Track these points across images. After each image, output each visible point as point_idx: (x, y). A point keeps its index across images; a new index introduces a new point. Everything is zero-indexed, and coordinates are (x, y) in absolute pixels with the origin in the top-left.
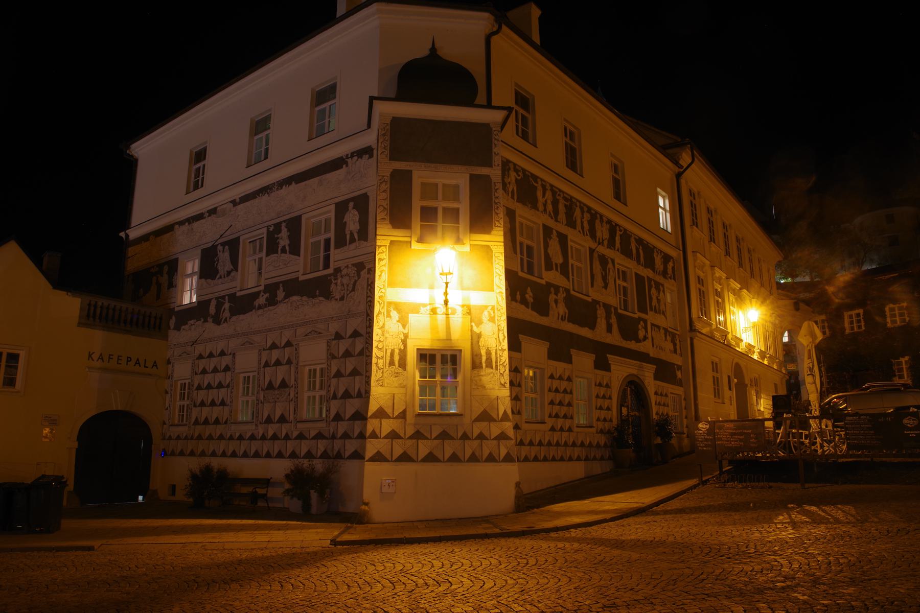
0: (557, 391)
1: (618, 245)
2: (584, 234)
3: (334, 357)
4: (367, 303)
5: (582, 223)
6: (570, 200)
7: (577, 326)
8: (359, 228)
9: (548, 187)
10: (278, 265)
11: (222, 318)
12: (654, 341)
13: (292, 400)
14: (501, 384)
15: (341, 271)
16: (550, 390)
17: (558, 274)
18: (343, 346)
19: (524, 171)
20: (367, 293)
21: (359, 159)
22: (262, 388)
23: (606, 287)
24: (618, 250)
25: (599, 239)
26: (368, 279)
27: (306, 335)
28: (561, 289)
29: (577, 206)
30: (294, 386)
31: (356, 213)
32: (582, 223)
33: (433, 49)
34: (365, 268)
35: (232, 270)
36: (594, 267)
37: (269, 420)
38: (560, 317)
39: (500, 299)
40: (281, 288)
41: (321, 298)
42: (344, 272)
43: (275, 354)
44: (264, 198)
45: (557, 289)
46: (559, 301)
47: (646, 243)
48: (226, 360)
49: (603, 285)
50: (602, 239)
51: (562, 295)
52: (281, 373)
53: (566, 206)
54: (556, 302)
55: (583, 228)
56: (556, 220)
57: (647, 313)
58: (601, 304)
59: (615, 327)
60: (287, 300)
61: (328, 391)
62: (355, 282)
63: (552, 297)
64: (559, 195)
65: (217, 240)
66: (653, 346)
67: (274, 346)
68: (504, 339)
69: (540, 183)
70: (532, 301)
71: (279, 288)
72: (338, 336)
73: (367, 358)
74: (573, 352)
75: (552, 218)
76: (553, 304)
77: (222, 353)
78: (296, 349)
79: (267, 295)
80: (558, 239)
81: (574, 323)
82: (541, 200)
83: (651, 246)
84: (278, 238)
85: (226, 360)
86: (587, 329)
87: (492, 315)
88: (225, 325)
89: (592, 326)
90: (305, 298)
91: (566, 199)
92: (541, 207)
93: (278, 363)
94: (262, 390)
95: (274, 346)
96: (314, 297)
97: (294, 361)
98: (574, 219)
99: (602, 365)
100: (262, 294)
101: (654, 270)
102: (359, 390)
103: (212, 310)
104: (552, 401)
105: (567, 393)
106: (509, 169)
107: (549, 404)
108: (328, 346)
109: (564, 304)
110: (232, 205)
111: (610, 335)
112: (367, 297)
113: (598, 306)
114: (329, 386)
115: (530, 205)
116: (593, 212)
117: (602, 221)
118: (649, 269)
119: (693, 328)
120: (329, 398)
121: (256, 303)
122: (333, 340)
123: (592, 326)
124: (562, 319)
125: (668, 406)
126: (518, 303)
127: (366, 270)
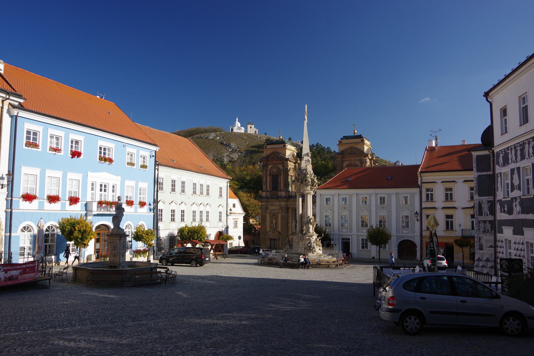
0: (517, 249)
5: (529, 151)
7: (525, 214)
16: (514, 249)
32: (529, 151)
45: (516, 198)
46: (517, 205)
54: (516, 206)
63: (514, 203)
74: (524, 229)
75: (515, 163)
76: (514, 207)
81: (524, 214)
82: (510, 157)
86: (531, 214)
92: (510, 161)
104: (515, 254)
105: (522, 251)
109: (519, 205)
124: (518, 214)
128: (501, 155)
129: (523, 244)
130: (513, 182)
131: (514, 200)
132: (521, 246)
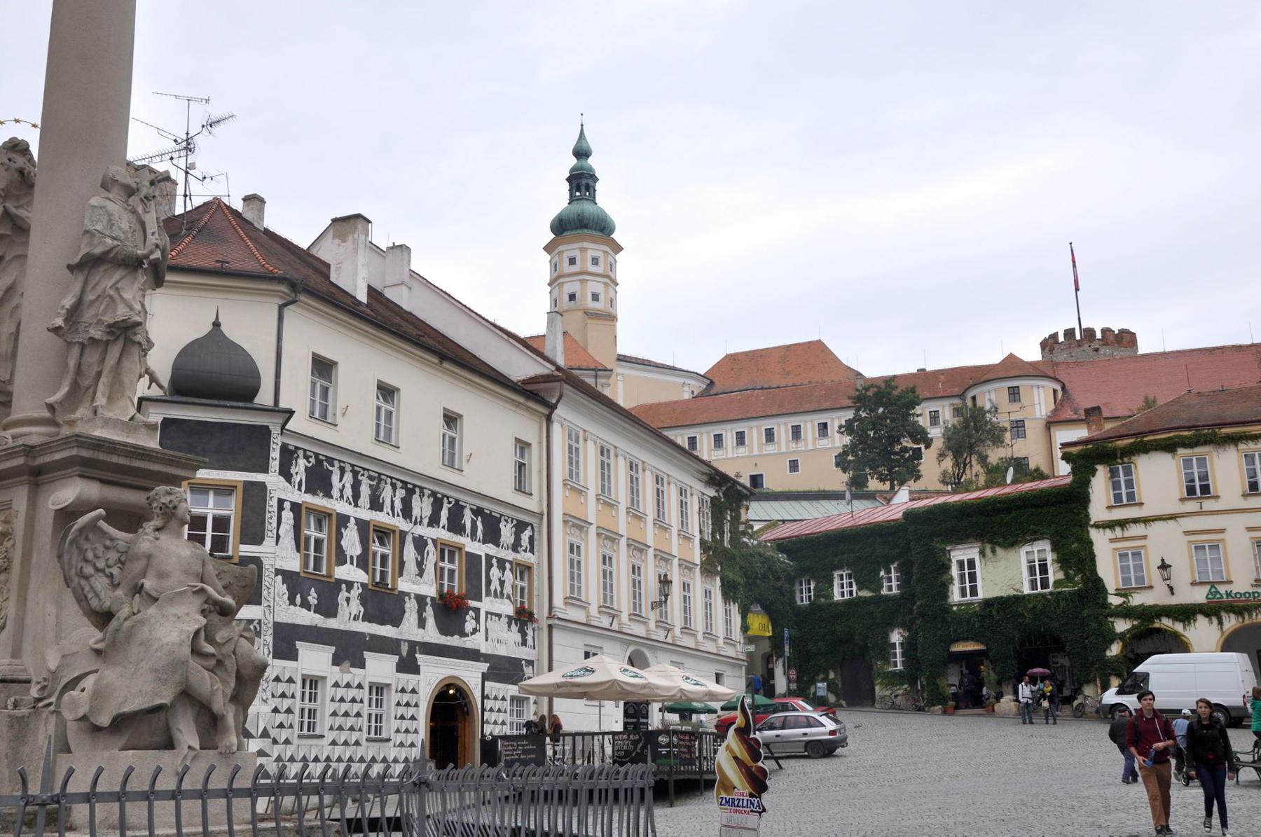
1: (444, 519)
2: (394, 516)
5: (392, 502)
6: (380, 477)
9: (348, 468)
12: (489, 633)
14: (263, 700)
16: (333, 700)
17: (353, 568)
19: (317, 455)
23: (421, 574)
24: (443, 527)
25: (416, 518)
28: (356, 584)
29: (386, 484)
32: (392, 502)
33: (216, 324)
36: (405, 553)
38: (352, 616)
39: (267, 613)
45: (350, 585)
47: (488, 512)
49: (418, 572)
50: (421, 517)
51: (356, 591)
53: (371, 486)
54: (348, 600)
55: (393, 508)
56: (356, 505)
57: (480, 600)
58: (412, 596)
59: (431, 622)
63: (343, 595)
64: (363, 475)
66: (487, 640)
68: (268, 655)
69: (336, 464)
70: (316, 602)
75: (350, 504)
80: (356, 527)
83: (496, 515)
87: (258, 628)
89: (396, 622)
91: (371, 478)
92: (335, 493)
98: (381, 501)
99: (408, 666)
101: (498, 545)
105: (356, 702)
106: (298, 457)
107: (331, 715)
109: (358, 602)
111: (422, 630)
113: (407, 599)
115: (321, 494)
116: (410, 486)
117: (422, 495)
118: (490, 545)
119: (553, 614)
123: (395, 619)
124: (354, 619)
125: (505, 712)
126: (298, 607)
128: (302, 463)
129: (360, 686)
130: (343, 543)
131: (344, 586)
132: (352, 693)
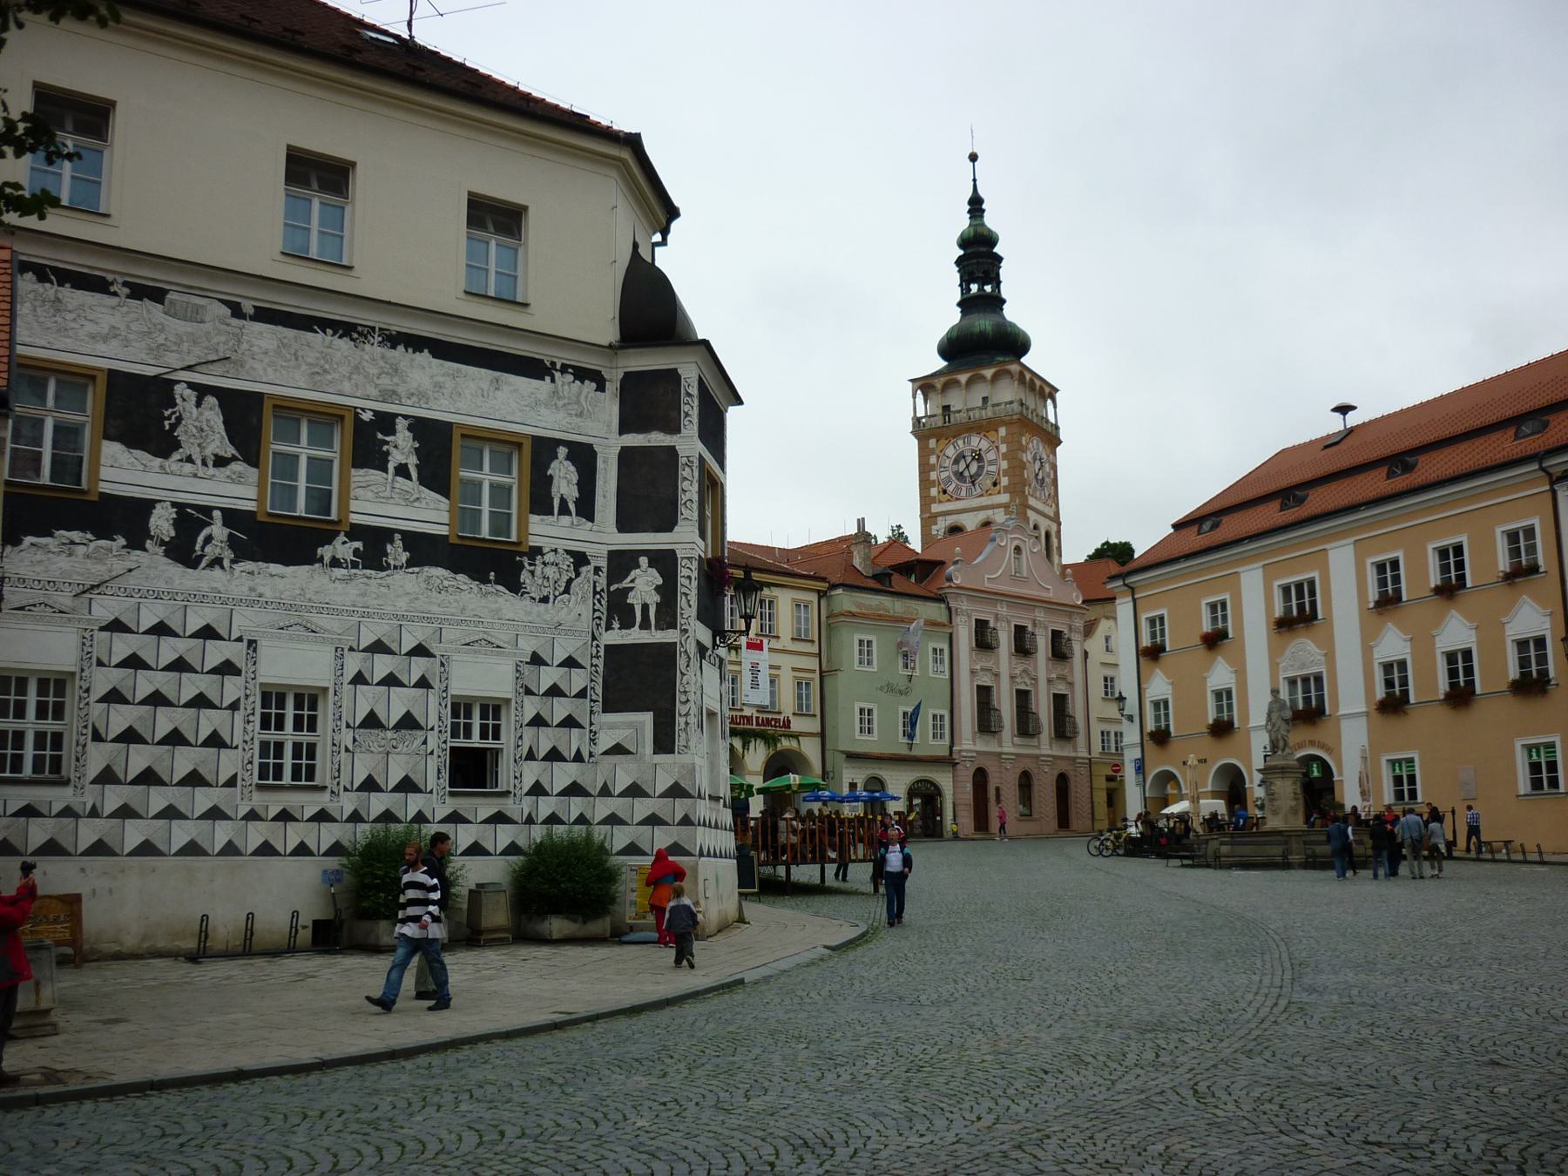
3: (529, 692)
4: (594, 619)
8: (577, 495)
10: (387, 494)
11: (202, 556)
13: (432, 753)
15: (543, 555)
18: (548, 677)
20: (594, 604)
21: (578, 382)
22: (347, 723)
26: (595, 583)
27: (468, 644)
30: (436, 728)
31: (572, 468)
34: (588, 563)
35: (234, 458)
37: (370, 785)
40: (399, 543)
41: (500, 588)
42: (549, 558)
43: (382, 666)
44: (344, 344)
48: (216, 653)
52: (398, 703)
60: (416, 569)
61: (518, 746)
62: (570, 581)
65: (176, 370)
67: (378, 647)
71: (392, 542)
72: (537, 660)
73: (592, 704)
77: (208, 633)
78: (442, 664)
79: (358, 544)
84: (387, 443)
85: (216, 653)
88: (217, 571)
90: (461, 577)
93: (391, 681)
94: (348, 726)
95: (378, 647)
96: (485, 581)
97: (436, 684)
100: (342, 538)
102: (578, 752)
103: (162, 522)
108: (517, 671)
110: (229, 312)
112: (595, 611)
114: (521, 737)
120: (521, 757)
121: (326, 552)
122: (527, 663)
127: (591, 568)
